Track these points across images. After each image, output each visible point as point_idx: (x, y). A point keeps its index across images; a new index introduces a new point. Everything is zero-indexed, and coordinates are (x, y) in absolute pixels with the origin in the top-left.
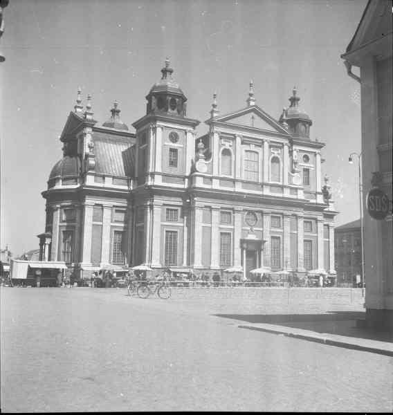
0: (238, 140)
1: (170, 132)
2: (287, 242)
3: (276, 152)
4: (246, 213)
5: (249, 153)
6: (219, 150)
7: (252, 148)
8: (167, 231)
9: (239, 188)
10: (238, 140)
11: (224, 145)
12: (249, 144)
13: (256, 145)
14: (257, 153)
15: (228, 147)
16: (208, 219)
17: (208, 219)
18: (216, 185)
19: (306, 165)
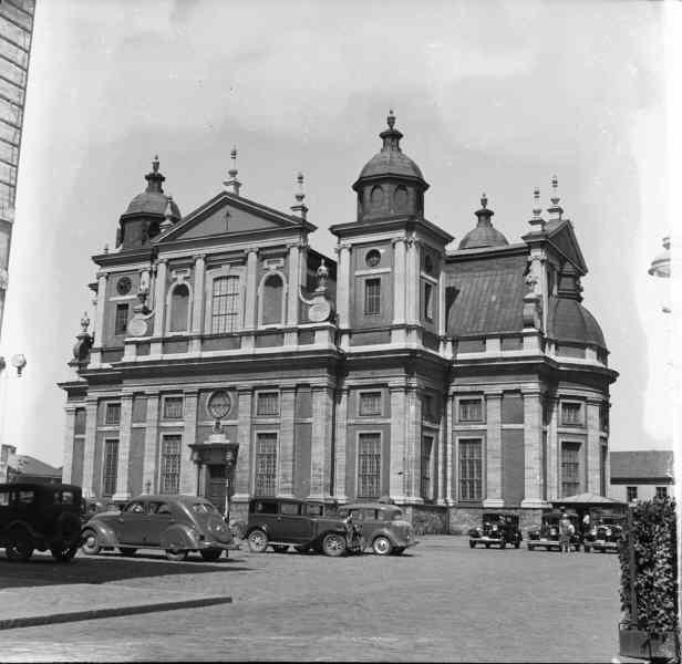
0: (200, 264)
1: (116, 280)
2: (286, 441)
3: (273, 267)
4: (210, 394)
5: (224, 282)
6: (166, 293)
7: (225, 270)
8: (107, 441)
9: (195, 352)
10: (200, 264)
11: (175, 279)
12: (220, 266)
13: (232, 265)
14: (237, 277)
15: (180, 282)
16: (139, 416)
17: (139, 416)
18: (156, 353)
19: (374, 271)
